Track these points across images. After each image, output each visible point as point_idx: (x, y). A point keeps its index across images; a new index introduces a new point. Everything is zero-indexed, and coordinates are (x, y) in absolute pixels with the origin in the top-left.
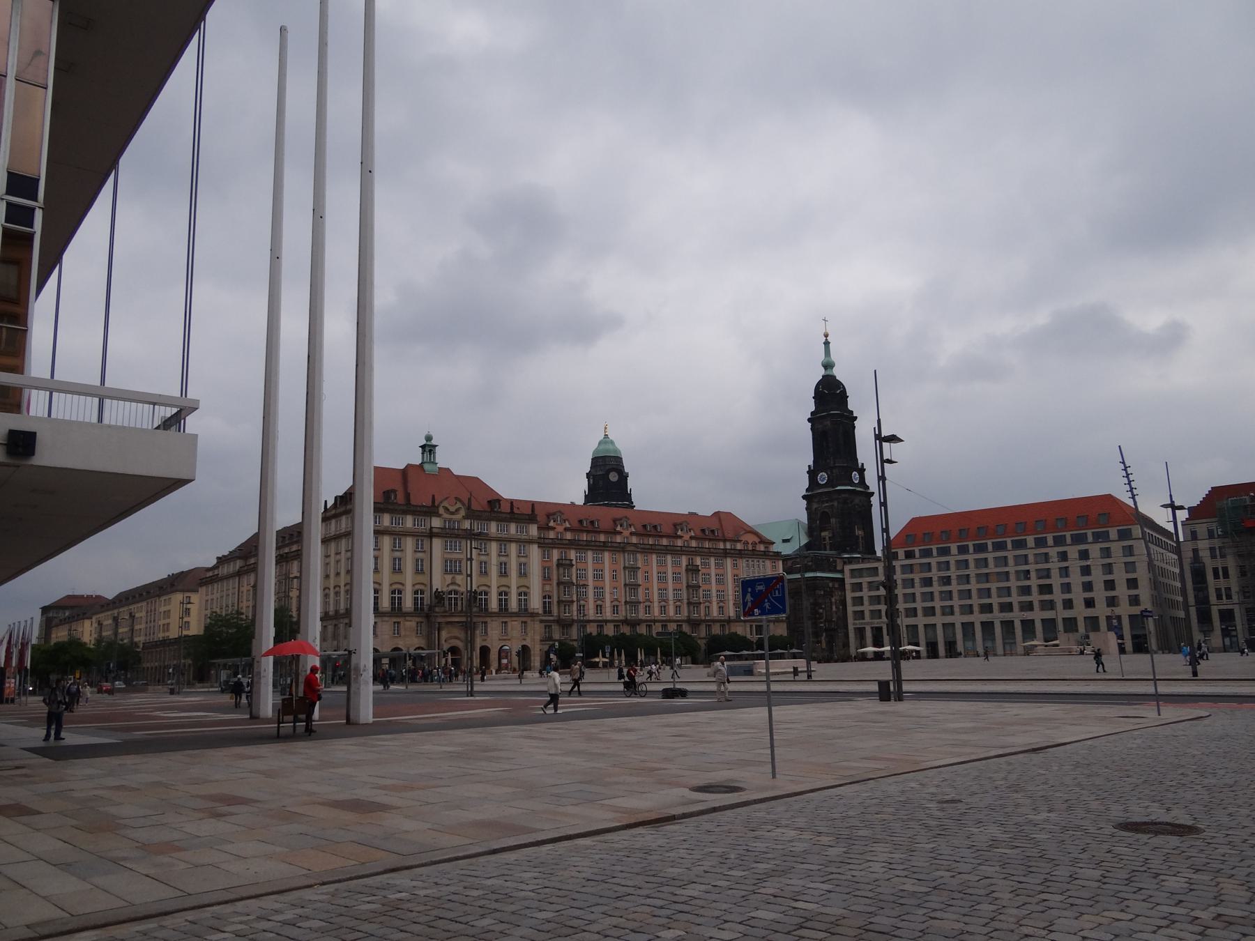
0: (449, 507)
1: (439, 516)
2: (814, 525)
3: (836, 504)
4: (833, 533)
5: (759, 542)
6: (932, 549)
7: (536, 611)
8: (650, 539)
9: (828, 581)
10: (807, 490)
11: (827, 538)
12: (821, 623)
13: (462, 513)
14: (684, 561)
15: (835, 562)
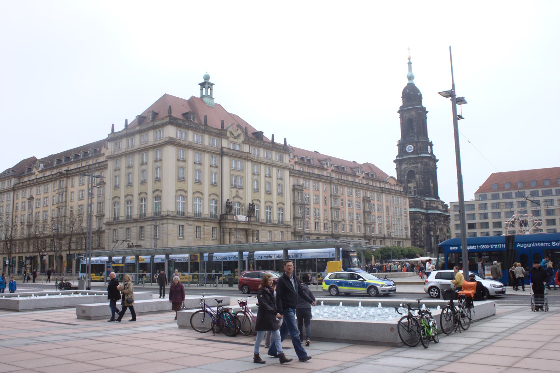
0: (233, 132)
1: (227, 138)
2: (403, 179)
3: (419, 165)
4: (417, 184)
5: (396, 185)
6: (512, 193)
7: (289, 223)
8: (342, 176)
9: (420, 215)
10: (397, 157)
11: (412, 188)
12: (418, 242)
13: (242, 138)
14: (361, 193)
15: (422, 202)
